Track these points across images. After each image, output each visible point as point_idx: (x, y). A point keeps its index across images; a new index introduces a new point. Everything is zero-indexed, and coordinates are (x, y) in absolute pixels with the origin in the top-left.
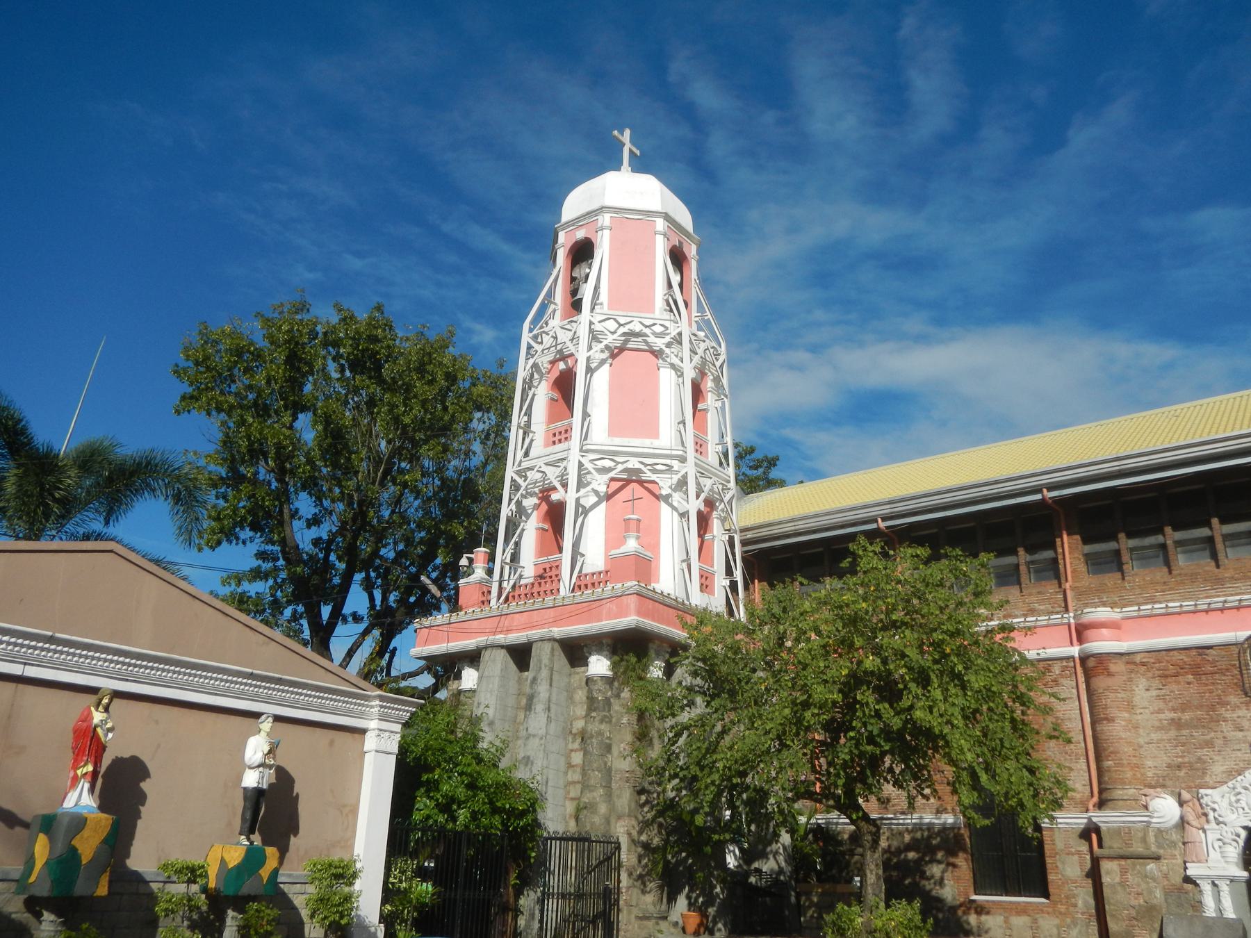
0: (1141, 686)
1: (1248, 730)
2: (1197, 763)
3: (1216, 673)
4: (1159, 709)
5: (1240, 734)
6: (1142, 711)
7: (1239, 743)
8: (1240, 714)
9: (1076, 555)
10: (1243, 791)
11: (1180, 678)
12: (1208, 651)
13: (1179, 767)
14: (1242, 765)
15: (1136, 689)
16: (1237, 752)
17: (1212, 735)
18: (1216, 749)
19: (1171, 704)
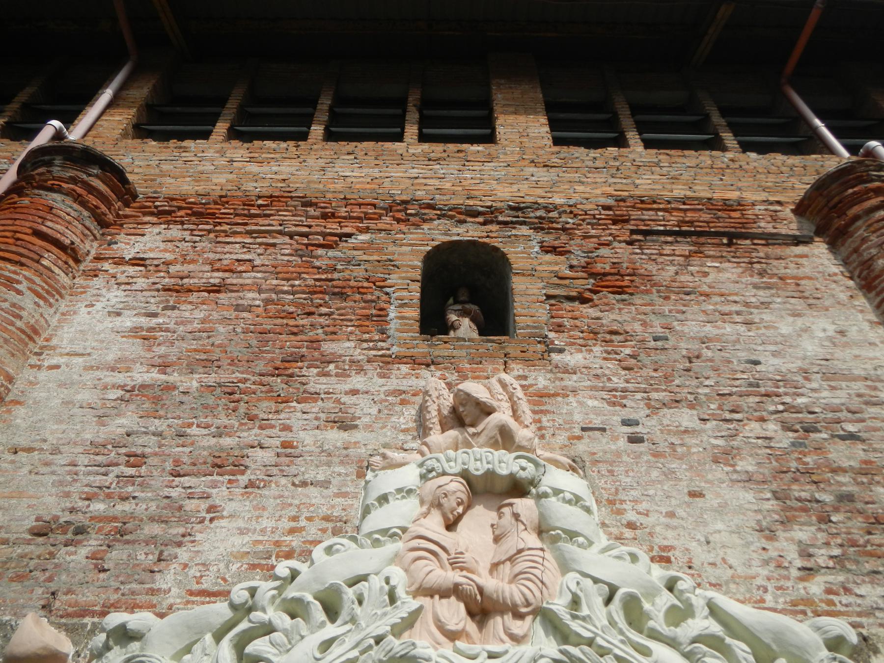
0: (99, 306)
1: (369, 427)
2: (152, 519)
3: (321, 292)
4: (120, 360)
5: (335, 437)
6: (62, 360)
7: (329, 464)
8: (359, 386)
9: (118, 118)
10: (282, 620)
11: (223, 297)
12: (320, 252)
13: (80, 531)
14: (312, 531)
15: (84, 310)
16: (312, 491)
17: (251, 435)
18: (243, 479)
19: (162, 350)
